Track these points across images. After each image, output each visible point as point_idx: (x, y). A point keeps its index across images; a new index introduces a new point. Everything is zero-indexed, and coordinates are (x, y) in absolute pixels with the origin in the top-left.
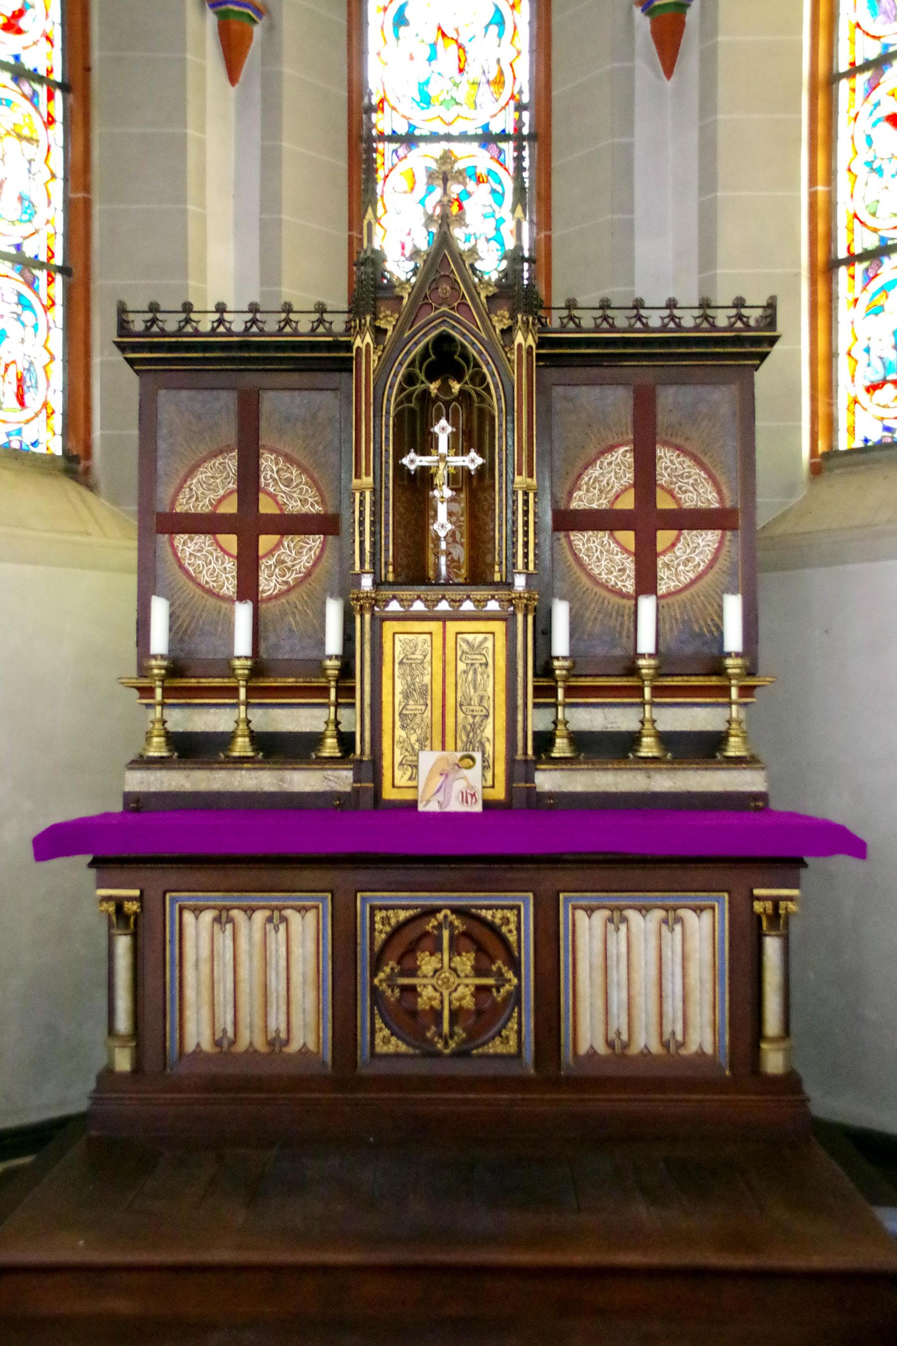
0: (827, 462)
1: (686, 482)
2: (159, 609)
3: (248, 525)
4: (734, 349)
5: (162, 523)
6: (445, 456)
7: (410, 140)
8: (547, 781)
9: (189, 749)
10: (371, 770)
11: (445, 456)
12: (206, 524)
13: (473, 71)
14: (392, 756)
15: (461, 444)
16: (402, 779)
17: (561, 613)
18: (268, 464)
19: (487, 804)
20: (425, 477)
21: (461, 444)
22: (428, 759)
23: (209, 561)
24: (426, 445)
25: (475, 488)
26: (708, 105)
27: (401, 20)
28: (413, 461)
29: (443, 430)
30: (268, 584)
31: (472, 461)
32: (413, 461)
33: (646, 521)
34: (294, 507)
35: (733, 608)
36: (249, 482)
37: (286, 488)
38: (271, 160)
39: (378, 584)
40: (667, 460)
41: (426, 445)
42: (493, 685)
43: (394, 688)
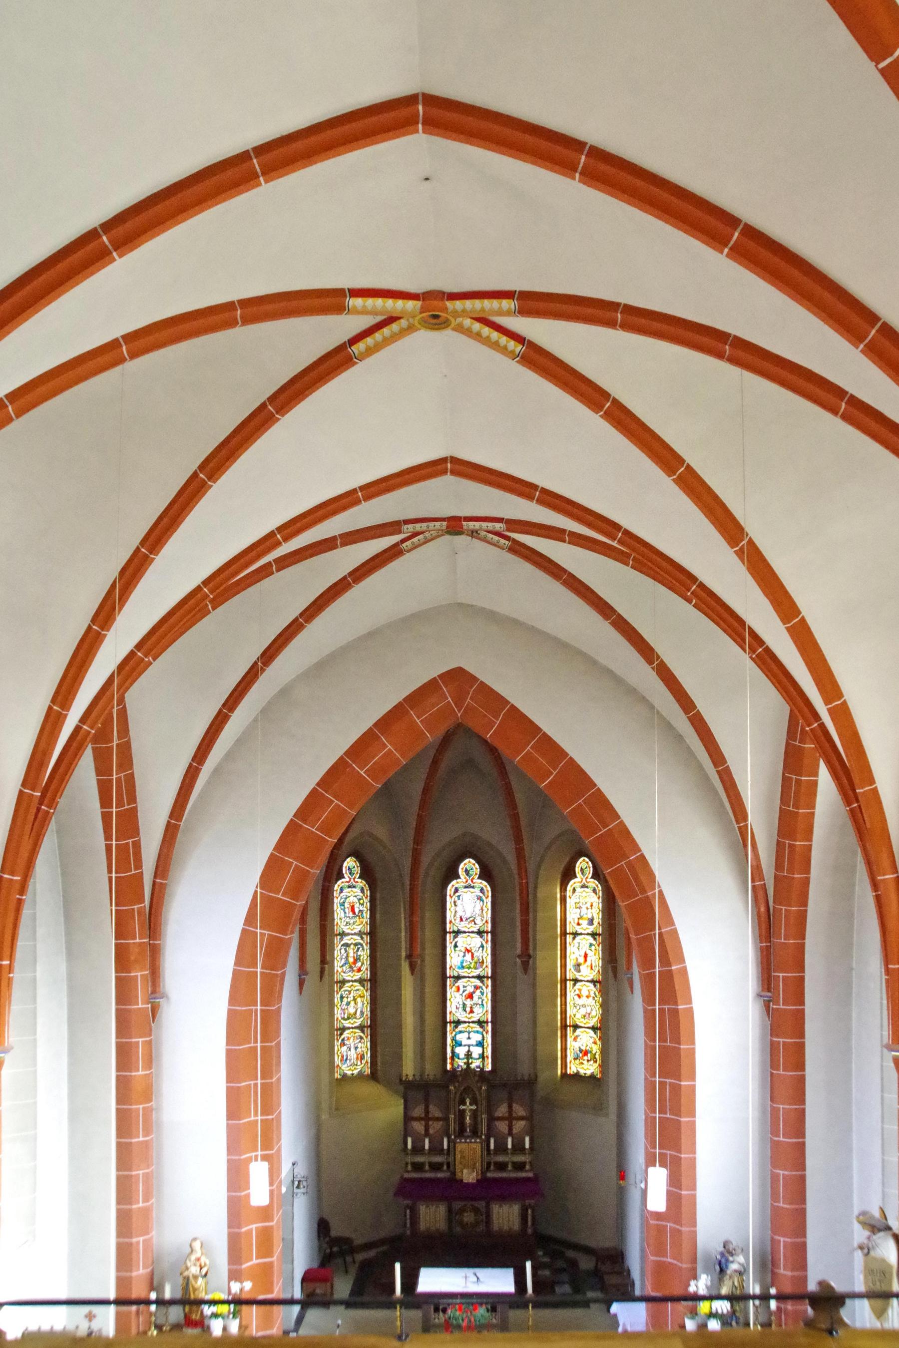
0: (565, 1075)
1: (519, 1110)
3: (427, 1118)
5: (408, 1118)
6: (468, 1107)
7: (458, 978)
8: (489, 1175)
9: (418, 1167)
10: (454, 1173)
11: (468, 1107)
12: (418, 1119)
13: (476, 959)
14: (458, 1170)
15: (471, 1104)
16: (460, 1174)
17: (492, 1141)
18: (432, 1108)
19: (478, 1180)
20: (464, 1111)
21: (471, 1104)
22: (465, 1171)
23: (419, 1127)
24: (465, 1104)
25: (475, 1114)
26: (534, 985)
27: (456, 946)
28: (462, 1107)
30: (431, 1131)
31: (474, 1107)
32: (462, 1107)
33: (510, 1118)
34: (436, 1115)
35: (527, 1139)
36: (427, 1112)
37: (435, 1112)
39: (455, 1137)
41: (465, 1104)
43: (458, 1156)
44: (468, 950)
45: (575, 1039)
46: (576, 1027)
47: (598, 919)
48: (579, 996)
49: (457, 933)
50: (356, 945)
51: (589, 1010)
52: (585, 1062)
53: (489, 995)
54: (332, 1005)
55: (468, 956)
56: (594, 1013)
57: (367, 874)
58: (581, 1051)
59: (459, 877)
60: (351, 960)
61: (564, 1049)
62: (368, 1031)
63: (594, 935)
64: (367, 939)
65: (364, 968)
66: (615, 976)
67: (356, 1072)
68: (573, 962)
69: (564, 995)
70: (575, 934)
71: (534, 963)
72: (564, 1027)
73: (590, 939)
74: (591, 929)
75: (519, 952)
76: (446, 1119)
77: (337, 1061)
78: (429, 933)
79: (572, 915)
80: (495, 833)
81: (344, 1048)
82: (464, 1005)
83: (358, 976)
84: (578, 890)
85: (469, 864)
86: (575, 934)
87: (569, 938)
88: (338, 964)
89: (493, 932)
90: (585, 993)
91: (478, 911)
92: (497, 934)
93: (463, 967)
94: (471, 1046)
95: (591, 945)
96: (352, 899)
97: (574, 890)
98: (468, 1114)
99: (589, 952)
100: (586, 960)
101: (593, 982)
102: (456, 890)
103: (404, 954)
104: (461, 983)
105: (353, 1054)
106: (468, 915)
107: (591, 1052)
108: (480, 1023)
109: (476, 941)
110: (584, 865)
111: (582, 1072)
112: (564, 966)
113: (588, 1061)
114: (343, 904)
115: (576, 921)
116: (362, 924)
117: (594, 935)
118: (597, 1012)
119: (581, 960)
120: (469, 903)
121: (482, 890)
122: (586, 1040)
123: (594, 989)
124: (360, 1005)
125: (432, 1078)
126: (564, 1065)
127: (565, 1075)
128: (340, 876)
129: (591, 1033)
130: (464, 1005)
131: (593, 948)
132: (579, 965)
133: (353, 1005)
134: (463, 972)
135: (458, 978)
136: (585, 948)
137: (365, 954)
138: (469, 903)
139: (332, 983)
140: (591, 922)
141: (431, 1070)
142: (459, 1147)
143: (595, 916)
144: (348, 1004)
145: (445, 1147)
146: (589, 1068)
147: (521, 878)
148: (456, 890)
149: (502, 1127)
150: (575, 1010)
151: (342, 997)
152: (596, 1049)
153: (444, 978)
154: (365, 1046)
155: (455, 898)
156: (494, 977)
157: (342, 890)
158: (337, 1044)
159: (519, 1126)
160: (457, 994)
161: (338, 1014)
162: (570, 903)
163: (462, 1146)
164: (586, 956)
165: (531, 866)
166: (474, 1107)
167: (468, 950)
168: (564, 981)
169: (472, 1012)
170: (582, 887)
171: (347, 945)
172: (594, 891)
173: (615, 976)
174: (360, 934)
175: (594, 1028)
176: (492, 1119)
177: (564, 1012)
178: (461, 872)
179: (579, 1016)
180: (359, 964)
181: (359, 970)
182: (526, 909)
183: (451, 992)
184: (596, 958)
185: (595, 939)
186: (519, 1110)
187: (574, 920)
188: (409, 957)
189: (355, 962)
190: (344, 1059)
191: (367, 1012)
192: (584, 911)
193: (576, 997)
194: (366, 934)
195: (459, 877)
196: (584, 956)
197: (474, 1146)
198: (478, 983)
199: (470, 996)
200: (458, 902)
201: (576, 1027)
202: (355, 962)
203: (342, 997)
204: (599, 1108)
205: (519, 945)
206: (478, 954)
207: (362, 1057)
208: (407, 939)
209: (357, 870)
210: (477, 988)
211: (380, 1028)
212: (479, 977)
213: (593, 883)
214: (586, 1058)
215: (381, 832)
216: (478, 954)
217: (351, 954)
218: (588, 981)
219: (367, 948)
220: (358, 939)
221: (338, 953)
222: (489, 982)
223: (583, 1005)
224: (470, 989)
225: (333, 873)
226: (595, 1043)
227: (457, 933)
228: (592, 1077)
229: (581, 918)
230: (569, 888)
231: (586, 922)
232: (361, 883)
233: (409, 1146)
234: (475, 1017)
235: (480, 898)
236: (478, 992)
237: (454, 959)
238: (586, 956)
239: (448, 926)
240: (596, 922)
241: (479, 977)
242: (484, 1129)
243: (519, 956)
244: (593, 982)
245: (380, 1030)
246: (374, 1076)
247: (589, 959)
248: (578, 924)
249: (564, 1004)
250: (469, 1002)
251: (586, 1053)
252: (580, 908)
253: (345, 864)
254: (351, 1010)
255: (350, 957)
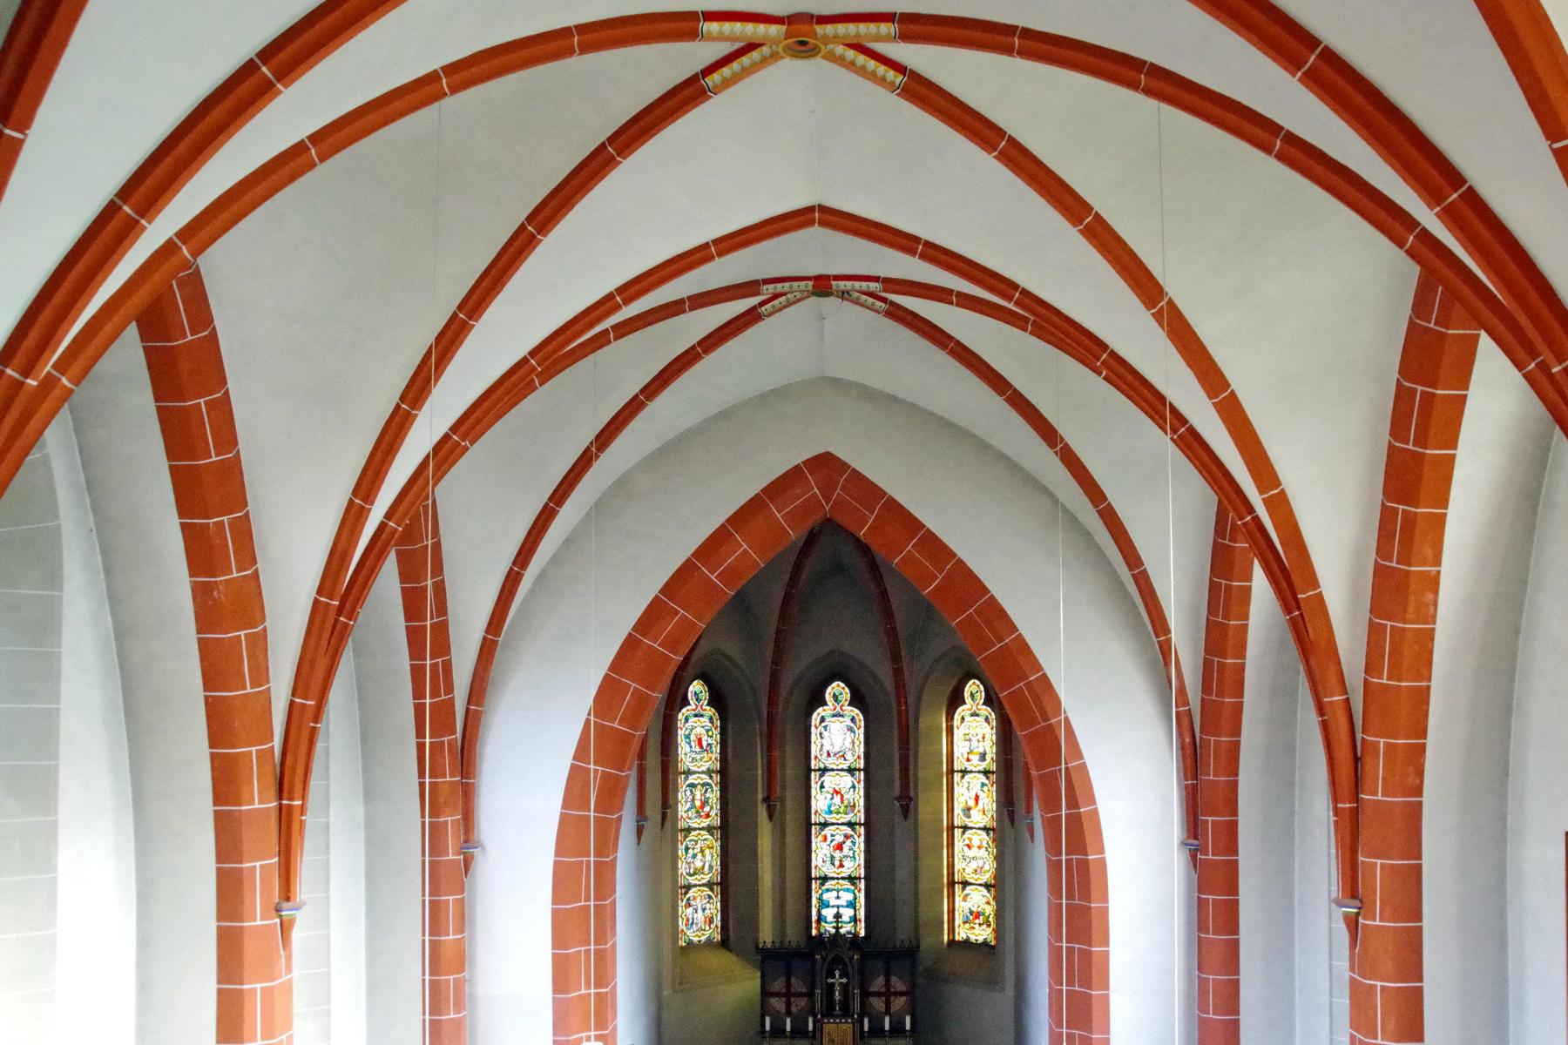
0: (952, 942)
1: (898, 984)
2: (768, 1020)
3: (788, 995)
4: (910, 953)
5: (765, 993)
6: (838, 980)
7: (825, 825)
11: (838, 980)
12: (777, 995)
17: (866, 1021)
18: (793, 980)
20: (833, 985)
23: (778, 1004)
24: (833, 976)
25: (845, 987)
27: (822, 787)
28: (830, 981)
29: (837, 973)
30: (794, 1010)
31: (844, 980)
32: (830, 981)
33: (888, 994)
35: (908, 1019)
36: (788, 985)
38: (783, 845)
40: (894, 979)
41: (833, 976)
42: (850, 1039)
44: (837, 793)
45: (965, 899)
46: (965, 884)
47: (991, 753)
49: (824, 771)
50: (703, 785)
51: (981, 863)
53: (862, 847)
54: (675, 858)
55: (837, 799)
56: (987, 867)
57: (717, 700)
58: (970, 914)
59: (825, 704)
60: (698, 803)
61: (952, 911)
62: (718, 889)
63: (986, 773)
64: (717, 778)
65: (713, 814)
66: (1012, 821)
67: (703, 938)
68: (963, 805)
69: (951, 844)
70: (964, 772)
71: (916, 808)
72: (952, 884)
73: (982, 778)
74: (983, 766)
75: (897, 792)
76: (810, 995)
77: (682, 925)
78: (791, 772)
79: (960, 749)
80: (869, 652)
81: (690, 910)
82: (832, 857)
83: (706, 823)
84: (968, 718)
85: (837, 689)
86: (964, 772)
87: (957, 777)
88: (682, 809)
89: (866, 770)
90: (976, 842)
91: (848, 745)
92: (872, 771)
93: (830, 812)
94: (840, 907)
95: (983, 785)
96: (699, 730)
98: (838, 988)
99: (981, 795)
101: (985, 829)
102: (823, 720)
103: (760, 796)
104: (828, 831)
105: (700, 917)
106: (837, 749)
108: (851, 879)
109: (846, 781)
110: (974, 688)
111: (973, 938)
112: (951, 810)
114: (688, 737)
116: (711, 761)
117: (986, 773)
118: (990, 866)
119: (972, 803)
120: (837, 734)
121: (853, 720)
122: (977, 899)
124: (708, 858)
125: (794, 945)
126: (952, 930)
127: (952, 942)
128: (685, 702)
129: (984, 891)
130: (832, 857)
132: (969, 809)
133: (700, 858)
134: (831, 818)
135: (825, 825)
136: (976, 788)
137: (714, 796)
138: (837, 734)
139: (675, 830)
140: (983, 757)
141: (793, 935)
142: (827, 1028)
143: (988, 750)
144: (694, 856)
145: (811, 1028)
146: (981, 934)
147: (899, 706)
148: (823, 720)
149: (878, 1004)
151: (687, 849)
152: (989, 910)
153: (808, 825)
154: (714, 908)
155: (821, 728)
156: (867, 825)
157: (687, 720)
158: (682, 904)
159: (899, 1003)
160: (824, 845)
161: (682, 868)
162: (958, 734)
163: (830, 1027)
164: (977, 798)
165: (912, 688)
166: (844, 980)
167: (837, 793)
168: (951, 828)
169: (841, 866)
171: (693, 786)
172: (987, 720)
173: (1012, 821)
174: (709, 772)
175: (987, 886)
176: (865, 994)
177: (951, 866)
178: (828, 697)
179: (968, 870)
180: (707, 809)
181: (708, 816)
182: (905, 744)
183: (816, 842)
184: (989, 801)
186: (898, 984)
188: (767, 799)
189: (702, 807)
190: (690, 923)
191: (717, 867)
192: (974, 744)
194: (717, 772)
195: (825, 704)
196: (974, 798)
197: (844, 1027)
198: (849, 831)
199: (840, 847)
200: (826, 734)
201: (965, 884)
202: (702, 807)
203: (687, 849)
204: (993, 981)
205: (897, 784)
206: (849, 796)
207: (711, 921)
208: (764, 776)
209: (705, 696)
210: (847, 837)
211: (732, 884)
212: (850, 825)
213: (985, 711)
215: (732, 648)
216: (849, 796)
217: (698, 796)
219: (716, 789)
220: (706, 778)
221: (683, 795)
222: (862, 830)
223: (974, 857)
224: (840, 839)
225: (676, 699)
227: (824, 771)
228: (985, 943)
229: (971, 752)
230: (957, 716)
232: (710, 711)
233: (768, 1028)
234: (845, 872)
235: (850, 729)
236: (849, 843)
237: (820, 803)
238: (977, 798)
239: (813, 762)
241: (850, 825)
242: (856, 1006)
243: (898, 799)
244: (985, 829)
245: (732, 890)
246: (725, 943)
249: (951, 855)
250: (837, 854)
251: (978, 915)
253: (691, 688)
254: (698, 864)
255: (697, 801)
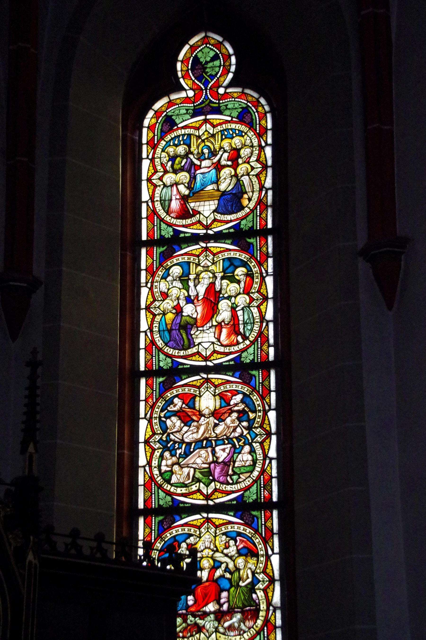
48: (186, 419)
52: (209, 623)
63: (239, 236)
73: (228, 249)
74: (228, 222)
84: (186, 121)
90: (207, 402)
95: (232, 264)
97: (170, 123)
100: (211, 308)
101: (240, 368)
107: (234, 584)
113: (220, 616)
115: (175, 205)
117: (239, 236)
123: (246, 389)
131: (240, 271)
140: (231, 201)
150: (168, 460)
164: (212, 298)
170: (196, 113)
172: (244, 117)
175: (241, 508)
185: (246, 248)
187: (166, 204)
193: (174, 423)
214: (211, 607)
218: (219, 369)
226: (250, 552)
229: (195, 193)
231: (213, 205)
238: (212, 298)
240: (249, 203)
244: (240, 368)
247: (224, 305)
248: (185, 213)
252: (192, 169)
